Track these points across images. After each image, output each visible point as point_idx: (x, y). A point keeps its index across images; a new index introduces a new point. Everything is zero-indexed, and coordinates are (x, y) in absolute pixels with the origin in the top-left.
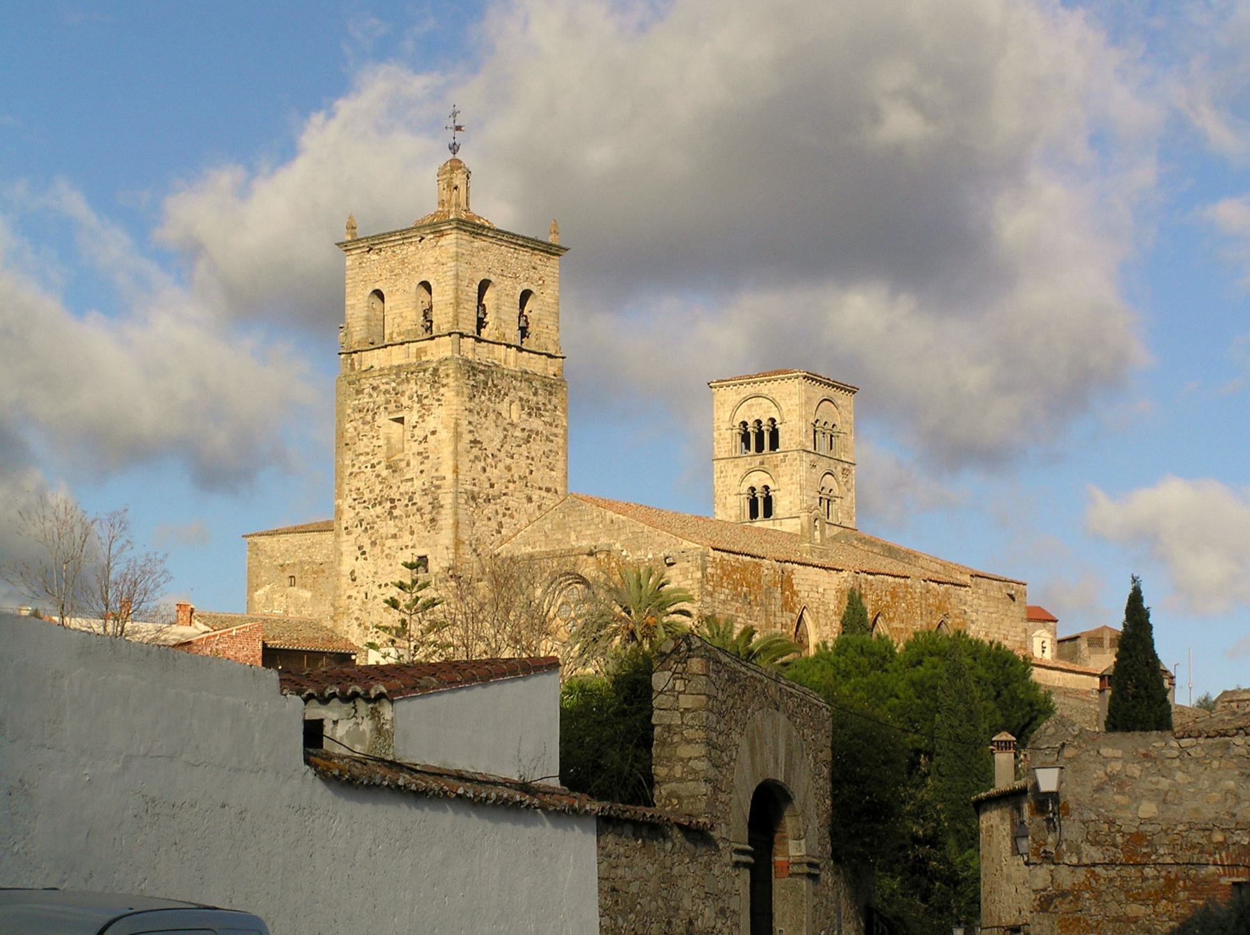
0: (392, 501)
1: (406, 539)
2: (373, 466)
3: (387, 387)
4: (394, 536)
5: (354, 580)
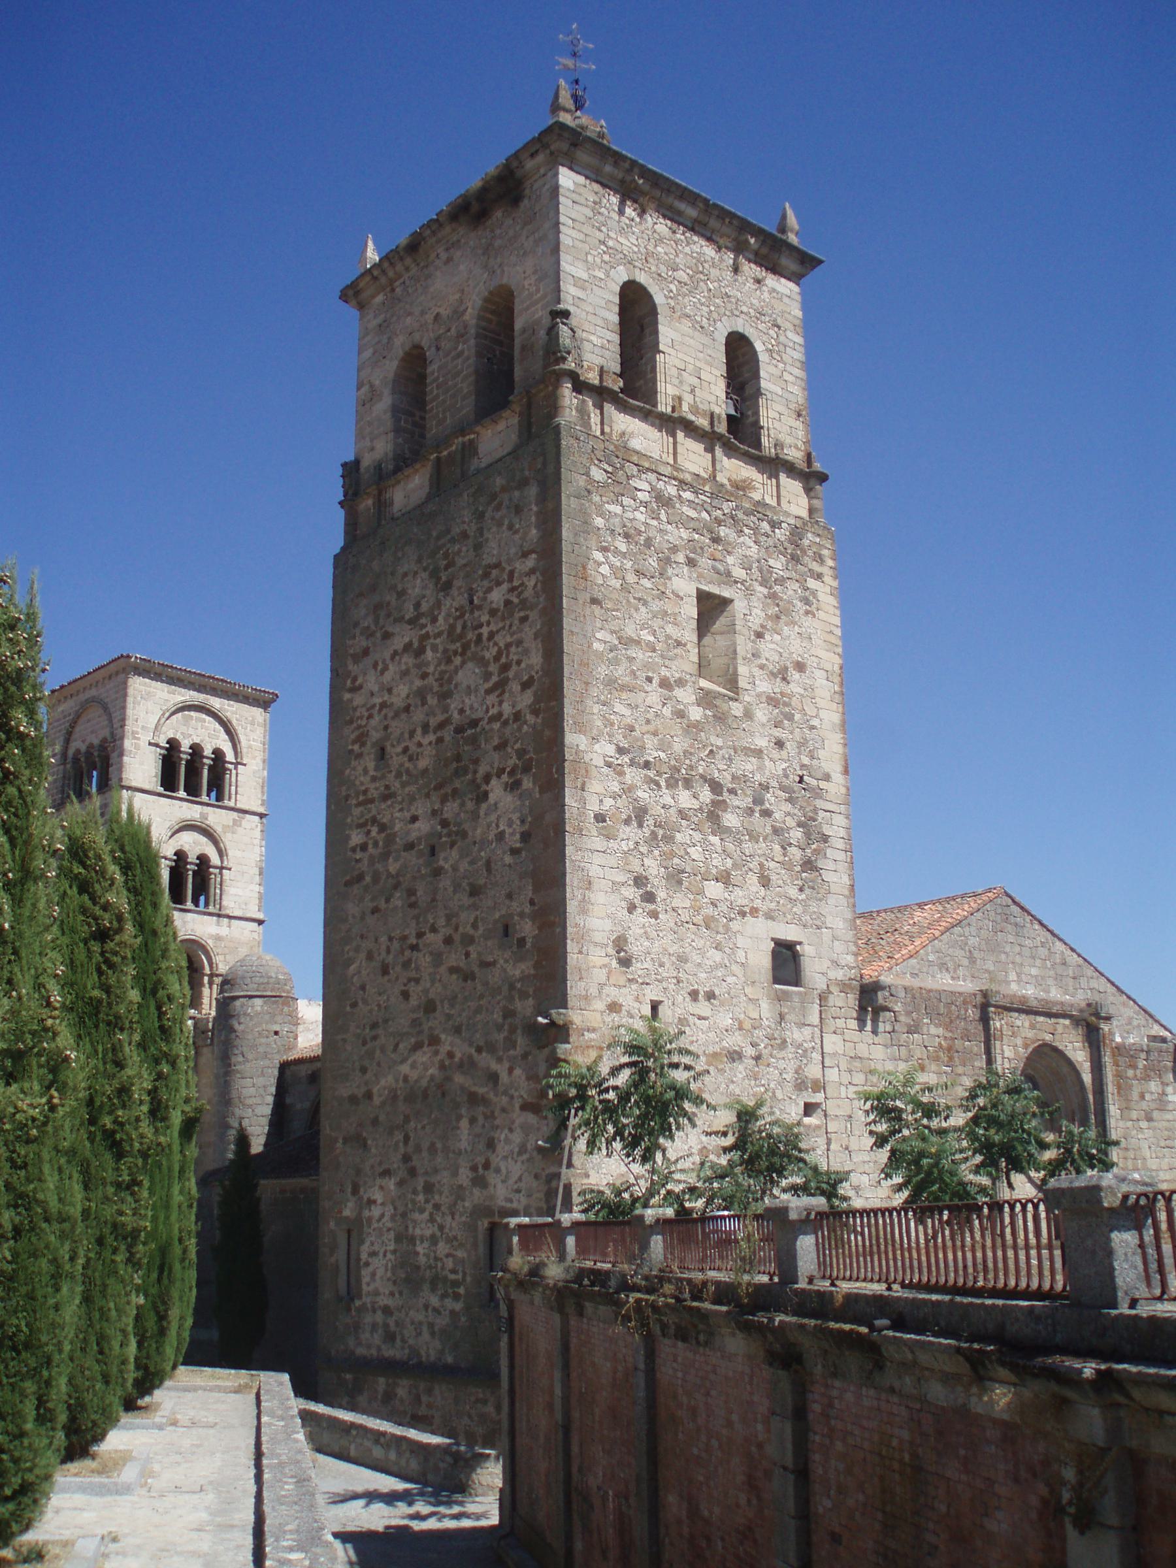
0: (716, 787)
1: (749, 890)
2: (665, 684)
3: (693, 514)
4: (724, 878)
5: (626, 962)
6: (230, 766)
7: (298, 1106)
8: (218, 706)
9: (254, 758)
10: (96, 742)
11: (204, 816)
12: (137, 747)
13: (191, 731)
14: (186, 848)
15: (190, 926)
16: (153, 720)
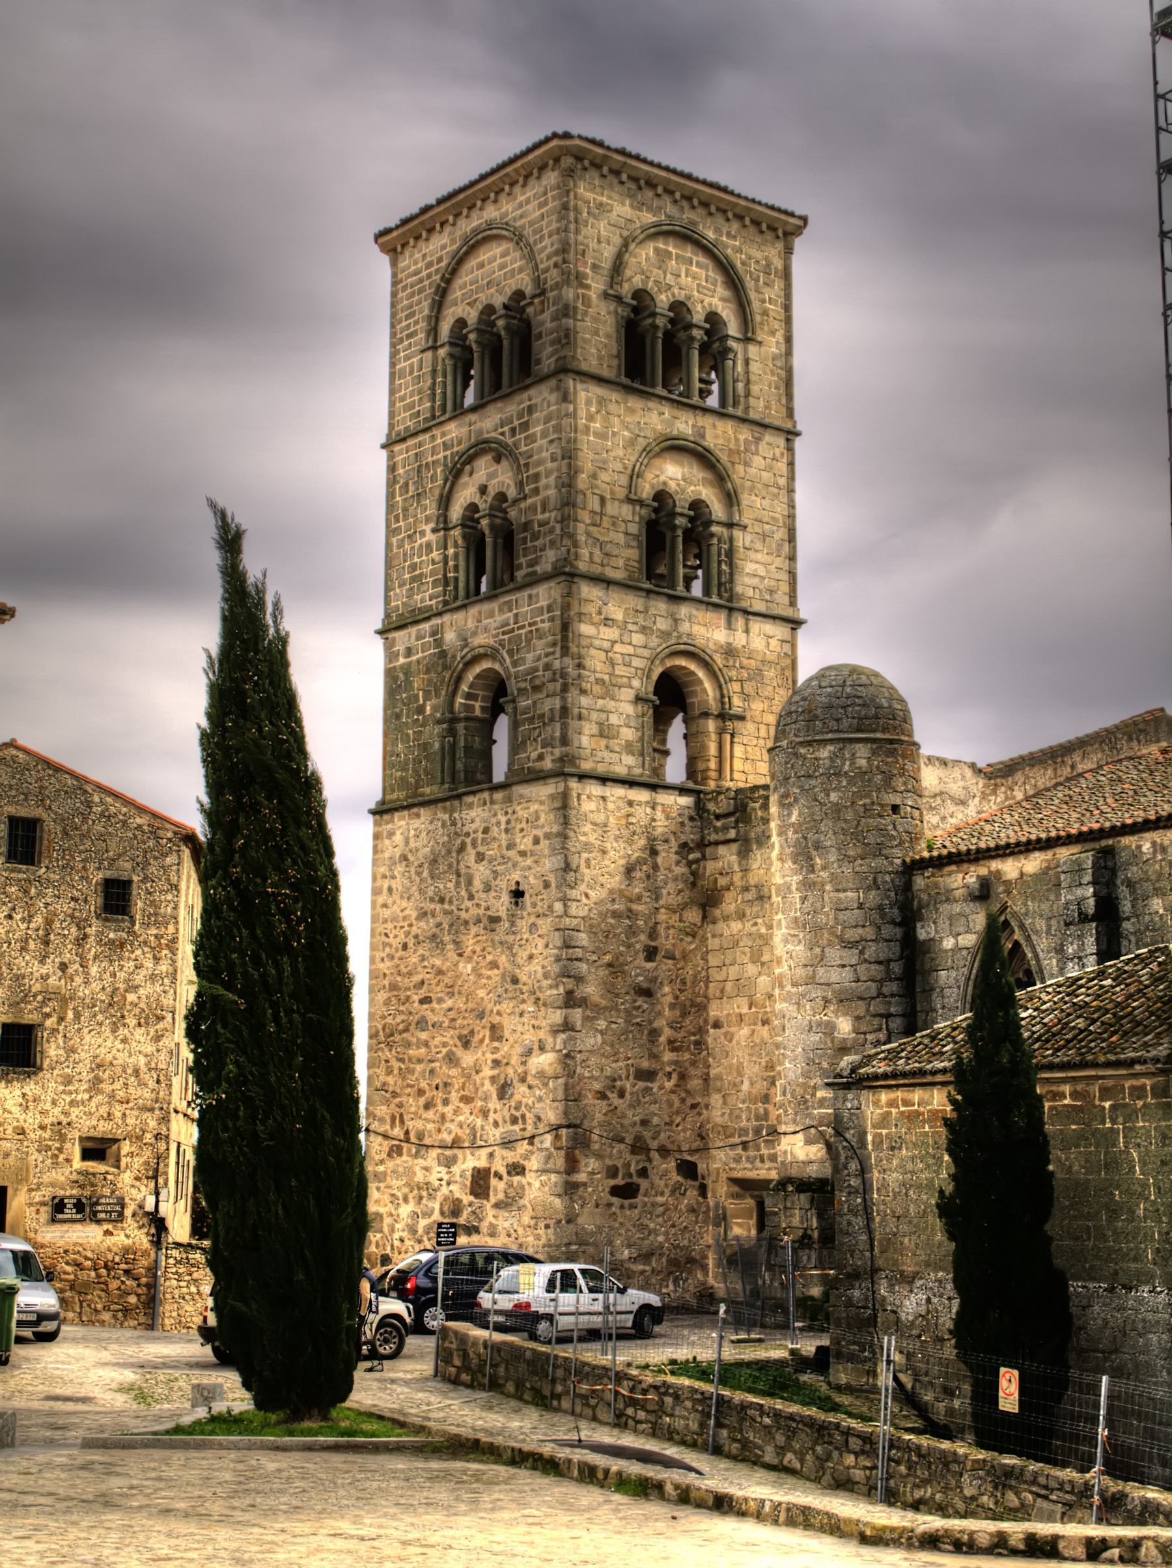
7: (948, 943)
9: (773, 333)
10: (499, 301)
13: (670, 279)
15: (685, 627)
16: (608, 253)
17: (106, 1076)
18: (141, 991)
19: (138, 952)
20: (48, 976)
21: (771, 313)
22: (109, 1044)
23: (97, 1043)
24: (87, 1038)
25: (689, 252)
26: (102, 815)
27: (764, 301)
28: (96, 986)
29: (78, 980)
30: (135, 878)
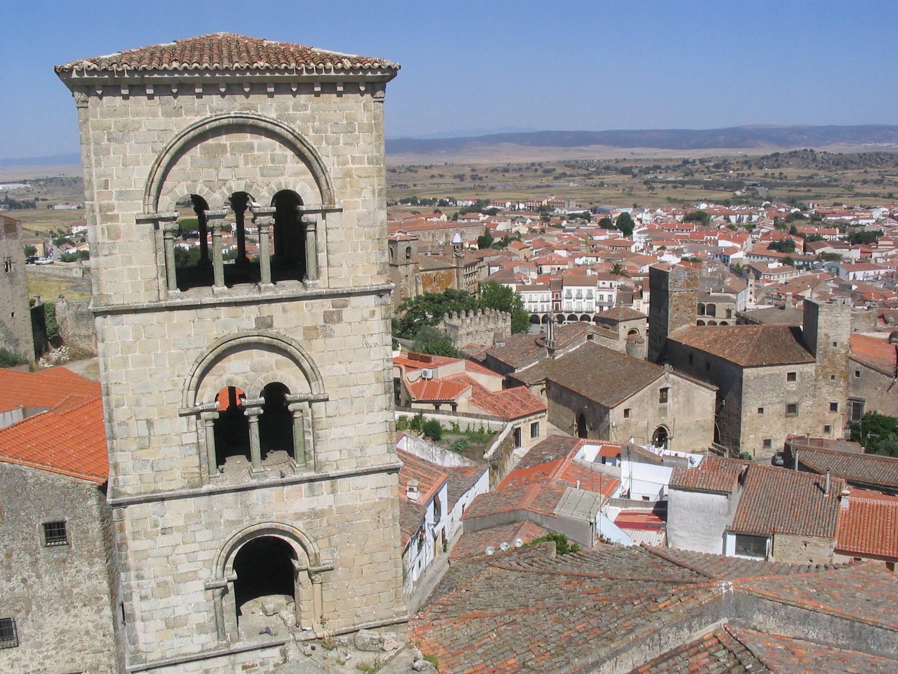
6: (311, 217)
8: (272, 115)
9: (359, 193)
11: (265, 323)
12: (113, 234)
13: (224, 173)
14: (239, 383)
15: (258, 510)
17: (66, 638)
18: (83, 586)
19: (77, 563)
20: (14, 589)
21: (354, 173)
22: (65, 620)
23: (55, 621)
24: (49, 619)
25: (248, 138)
26: (36, 483)
27: (345, 163)
28: (50, 588)
29: (36, 587)
30: (67, 519)
